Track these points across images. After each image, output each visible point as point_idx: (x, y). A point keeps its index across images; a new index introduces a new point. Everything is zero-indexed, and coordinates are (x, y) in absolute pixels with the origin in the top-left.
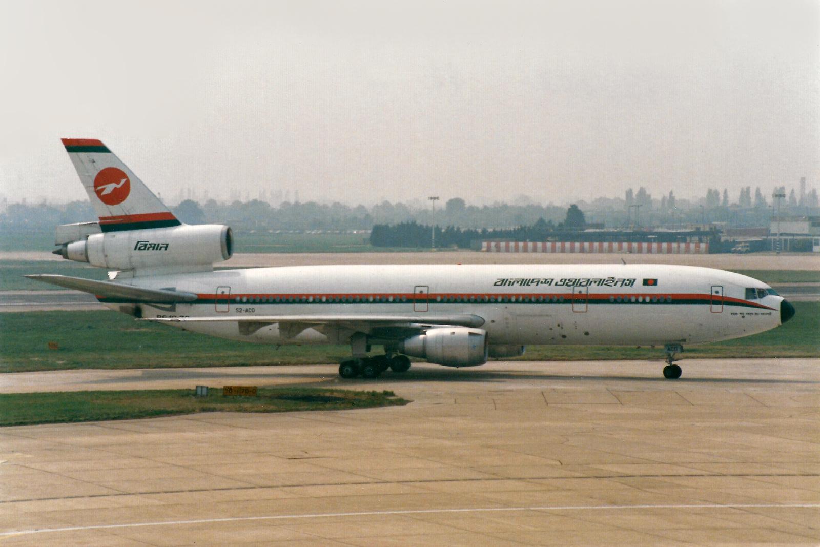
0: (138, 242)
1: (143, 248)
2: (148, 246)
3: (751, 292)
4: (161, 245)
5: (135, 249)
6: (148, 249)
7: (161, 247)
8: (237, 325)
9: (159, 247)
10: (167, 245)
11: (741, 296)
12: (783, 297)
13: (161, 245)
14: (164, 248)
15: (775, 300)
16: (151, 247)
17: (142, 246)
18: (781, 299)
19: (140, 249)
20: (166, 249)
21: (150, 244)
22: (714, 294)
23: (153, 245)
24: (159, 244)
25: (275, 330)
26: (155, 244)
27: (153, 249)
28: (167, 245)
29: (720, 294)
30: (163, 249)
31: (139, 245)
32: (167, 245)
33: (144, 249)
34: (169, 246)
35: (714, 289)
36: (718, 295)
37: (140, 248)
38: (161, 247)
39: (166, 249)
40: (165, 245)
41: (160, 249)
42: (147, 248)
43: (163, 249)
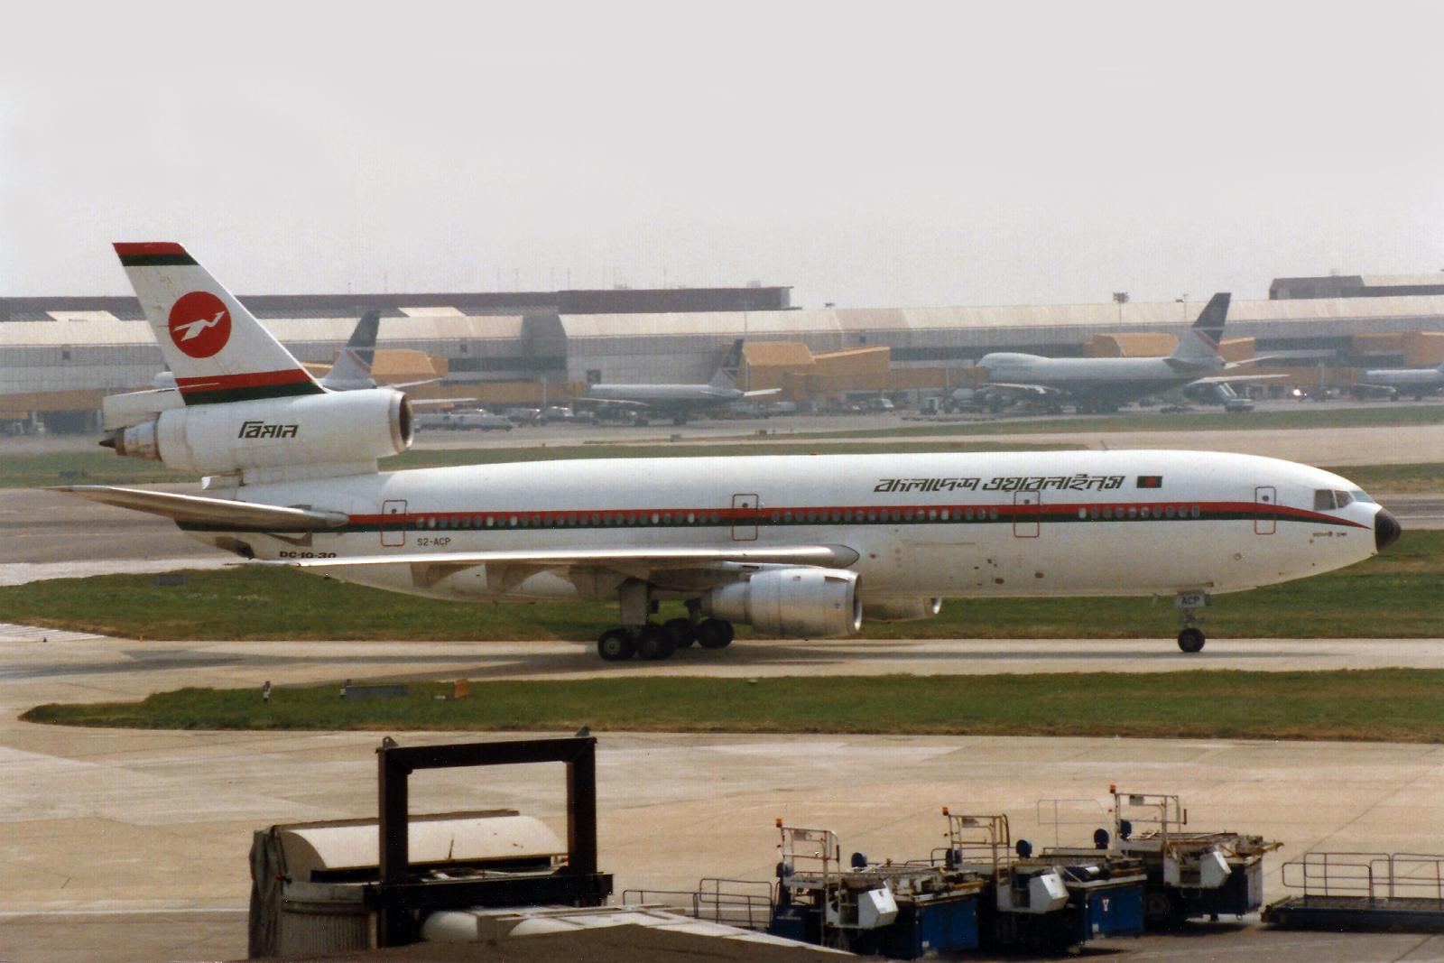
0: (246, 423)
1: (253, 434)
2: (263, 430)
3: (1324, 496)
4: (284, 429)
5: (240, 436)
6: (263, 436)
7: (285, 432)
8: (409, 567)
9: (282, 433)
10: (296, 427)
11: (1308, 506)
12: (1379, 502)
13: (284, 429)
14: (291, 434)
15: (1369, 509)
16: (268, 432)
17: (251, 431)
18: (1375, 508)
19: (248, 435)
20: (293, 436)
21: (266, 427)
22: (1260, 501)
23: (271, 429)
24: (281, 427)
25: (475, 578)
26: (274, 427)
27: (271, 436)
28: (296, 427)
29: (1270, 502)
30: (289, 435)
31: (247, 430)
32: (296, 427)
33: (256, 436)
34: (298, 430)
35: (1261, 493)
36: (1266, 503)
37: (248, 433)
38: (286, 432)
39: (293, 436)
40: (292, 429)
41: (284, 436)
42: (260, 435)
43: (289, 435)
